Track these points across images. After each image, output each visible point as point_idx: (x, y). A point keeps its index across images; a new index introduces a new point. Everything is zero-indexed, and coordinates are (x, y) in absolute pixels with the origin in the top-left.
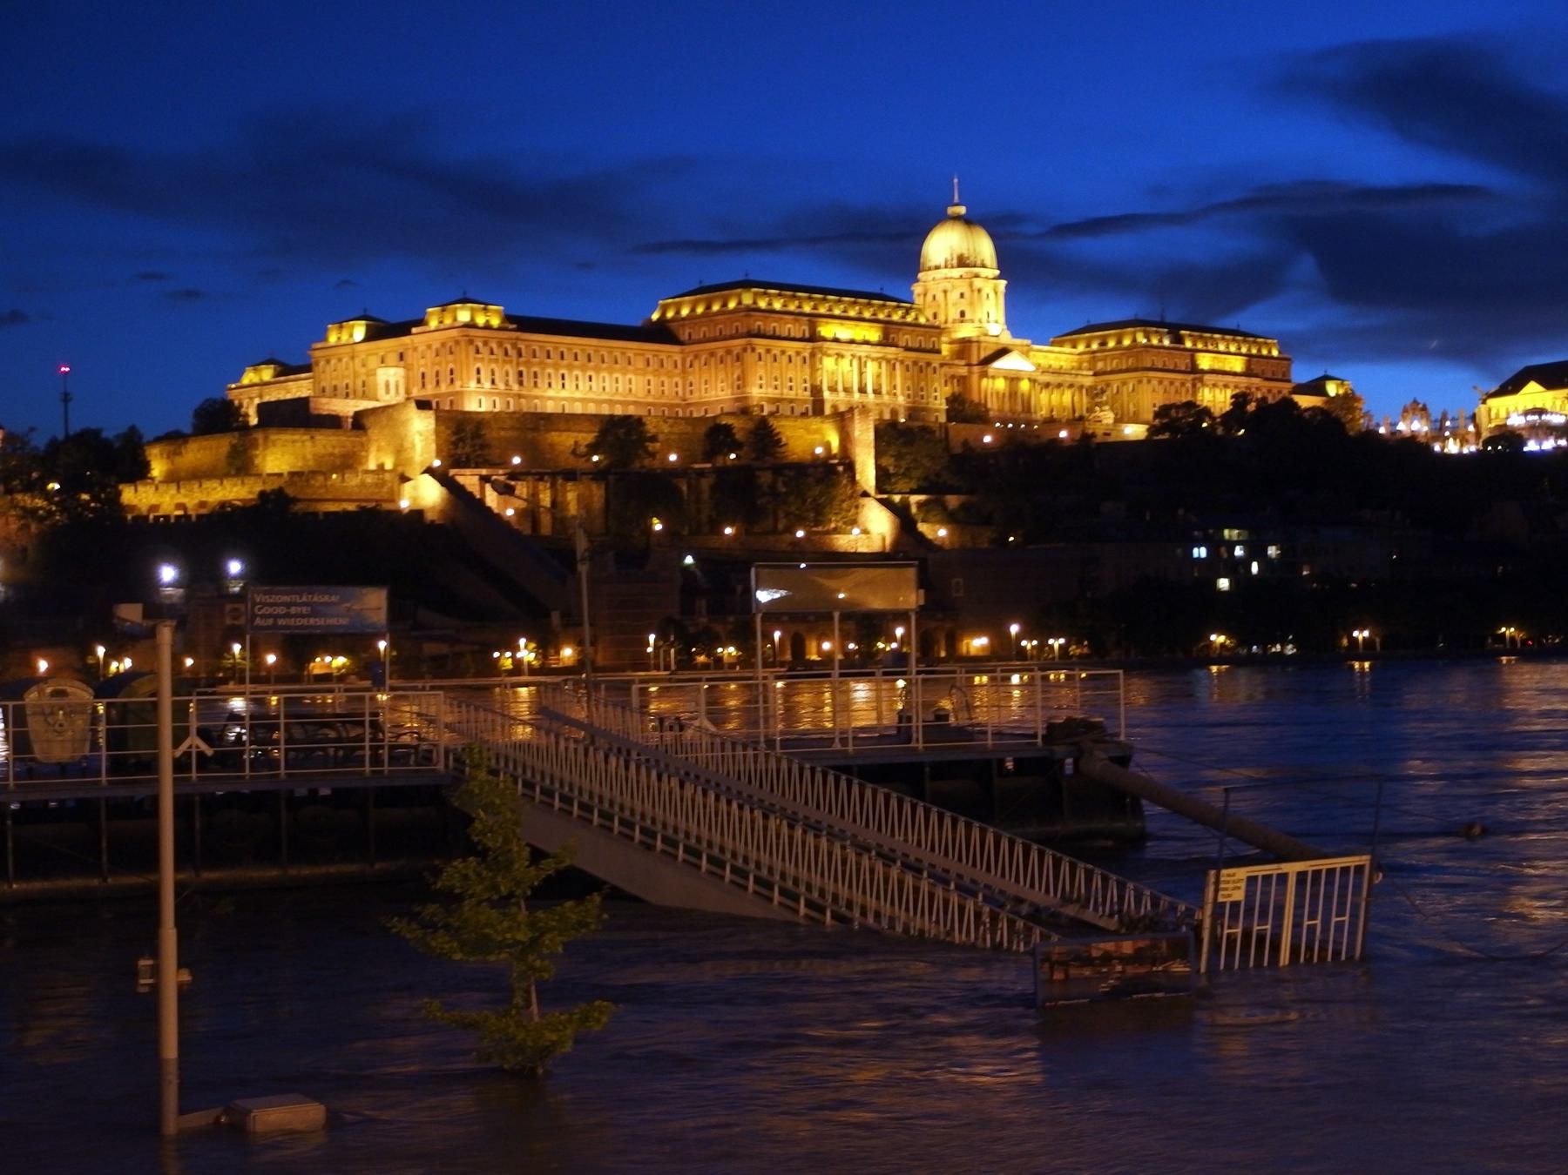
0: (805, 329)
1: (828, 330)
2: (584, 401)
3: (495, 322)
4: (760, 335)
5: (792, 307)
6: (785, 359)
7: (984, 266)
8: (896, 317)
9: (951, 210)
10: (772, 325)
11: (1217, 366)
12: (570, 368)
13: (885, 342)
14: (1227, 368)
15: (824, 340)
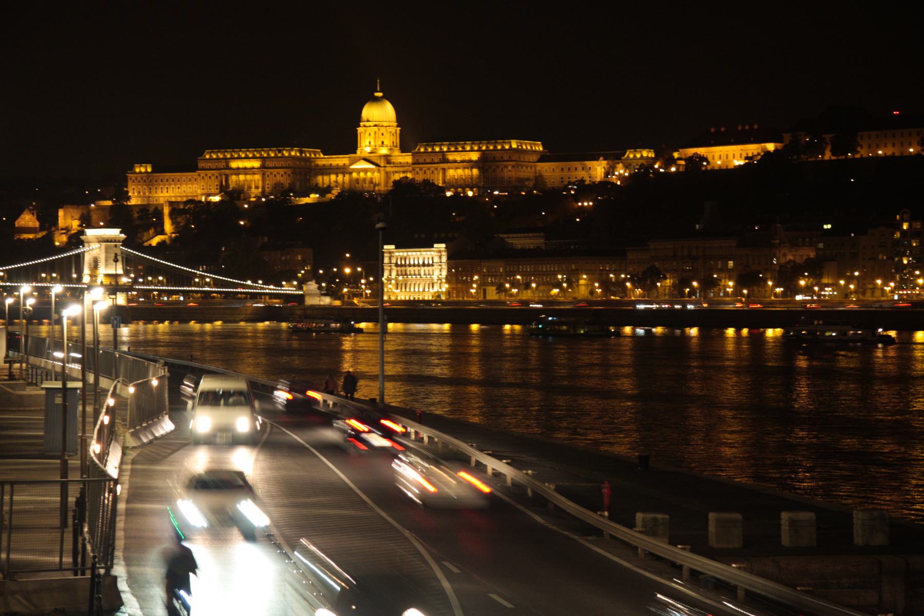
0: (223, 164)
1: (234, 164)
2: (175, 197)
3: (143, 170)
4: (203, 169)
5: (221, 156)
6: (213, 178)
7: (368, 121)
8: (273, 155)
9: (377, 94)
10: (209, 165)
11: (459, 158)
12: (170, 185)
13: (263, 167)
14: (467, 158)
15: (231, 169)
